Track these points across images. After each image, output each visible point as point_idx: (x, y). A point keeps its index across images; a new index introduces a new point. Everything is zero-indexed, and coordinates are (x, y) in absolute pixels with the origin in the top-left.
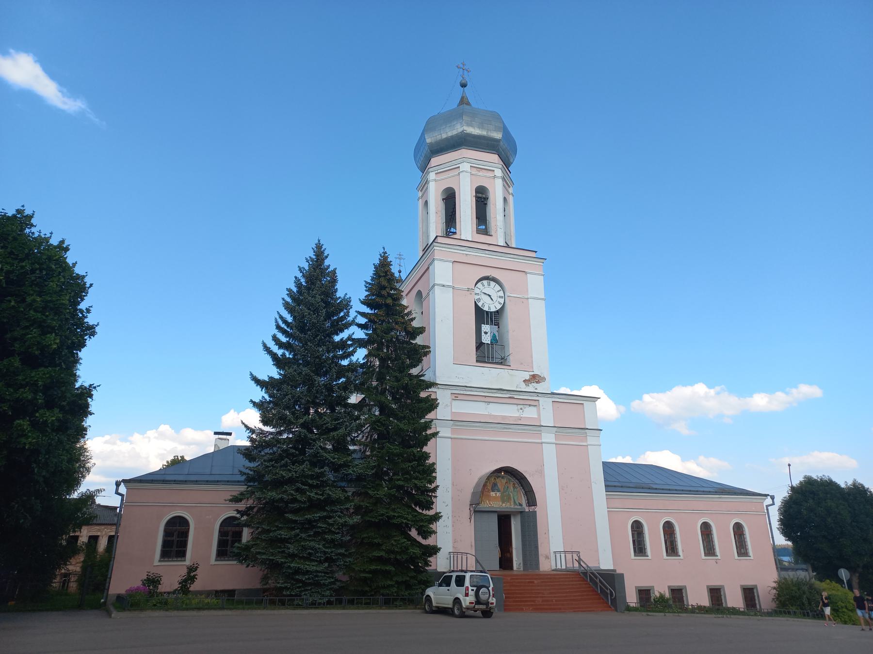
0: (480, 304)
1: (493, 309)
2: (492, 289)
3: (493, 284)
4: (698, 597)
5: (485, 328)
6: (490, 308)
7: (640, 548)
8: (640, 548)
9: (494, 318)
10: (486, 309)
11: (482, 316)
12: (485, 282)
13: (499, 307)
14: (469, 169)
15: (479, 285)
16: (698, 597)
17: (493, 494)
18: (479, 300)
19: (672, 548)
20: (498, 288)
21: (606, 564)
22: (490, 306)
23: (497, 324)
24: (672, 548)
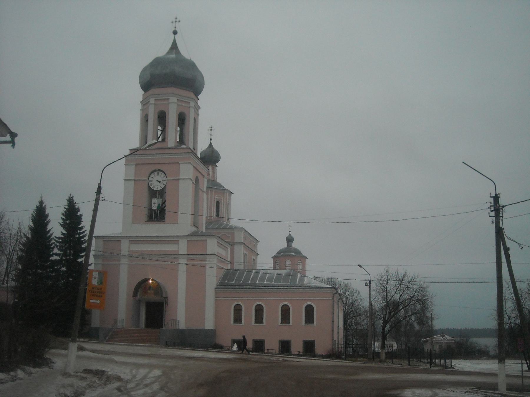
0: (152, 187)
1: (159, 189)
2: (159, 177)
3: (160, 173)
4: (272, 345)
5: (155, 200)
6: (157, 188)
7: (238, 319)
8: (238, 319)
9: (161, 194)
10: (155, 189)
11: (153, 194)
12: (156, 173)
13: (163, 186)
14: (153, 102)
15: (152, 175)
16: (272, 345)
17: (149, 291)
18: (151, 184)
19: (259, 318)
20: (163, 175)
21: (209, 325)
22: (157, 187)
23: (162, 197)
24: (259, 318)
